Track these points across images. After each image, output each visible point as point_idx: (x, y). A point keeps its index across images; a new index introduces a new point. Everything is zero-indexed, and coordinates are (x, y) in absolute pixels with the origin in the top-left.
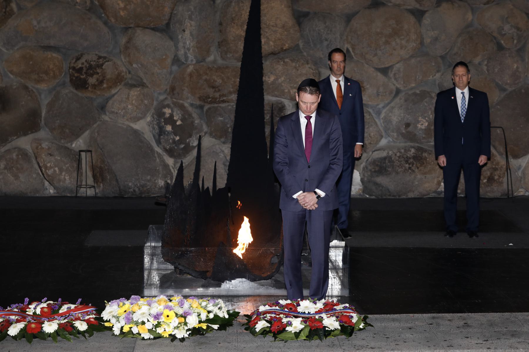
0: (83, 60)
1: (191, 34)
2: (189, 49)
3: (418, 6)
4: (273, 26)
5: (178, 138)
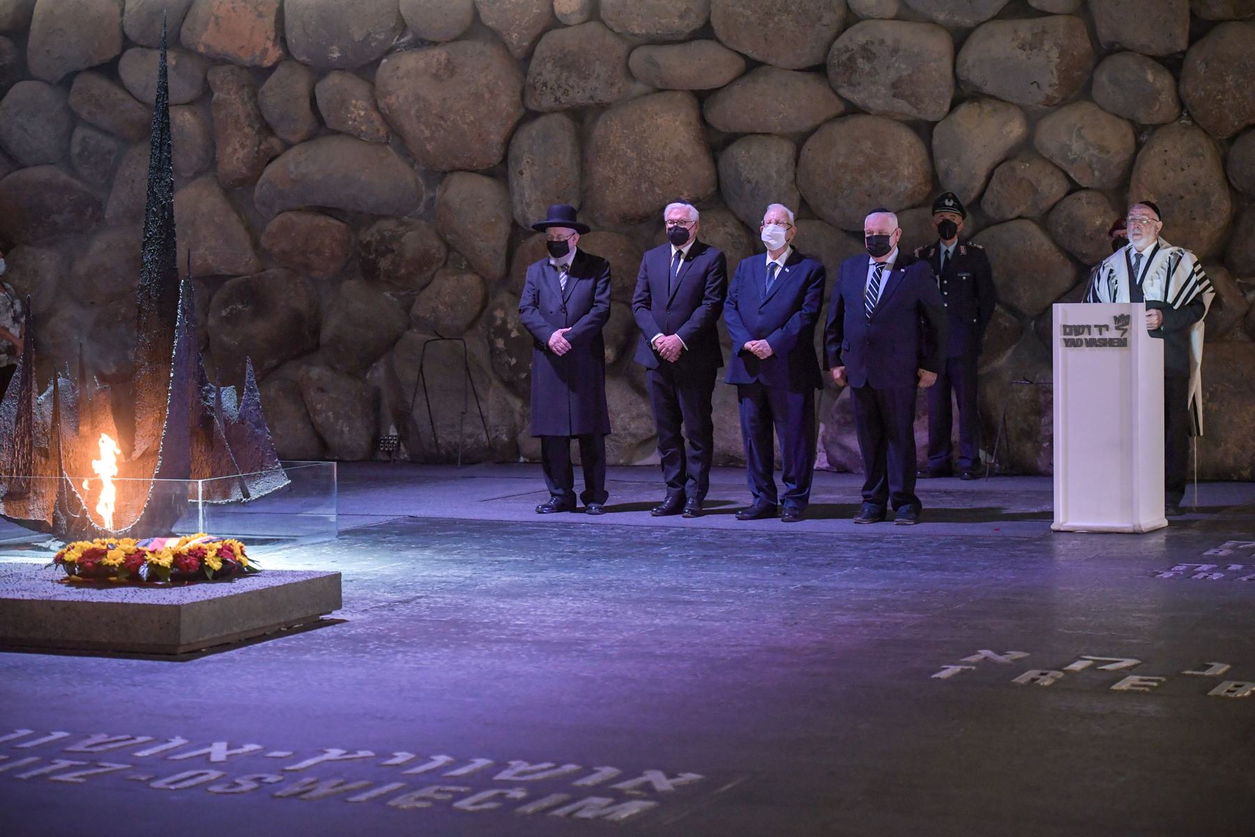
0: (374, 229)
1: (533, 178)
2: (529, 205)
3: (915, 112)
4: (658, 160)
5: (514, 361)
